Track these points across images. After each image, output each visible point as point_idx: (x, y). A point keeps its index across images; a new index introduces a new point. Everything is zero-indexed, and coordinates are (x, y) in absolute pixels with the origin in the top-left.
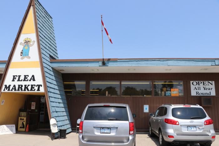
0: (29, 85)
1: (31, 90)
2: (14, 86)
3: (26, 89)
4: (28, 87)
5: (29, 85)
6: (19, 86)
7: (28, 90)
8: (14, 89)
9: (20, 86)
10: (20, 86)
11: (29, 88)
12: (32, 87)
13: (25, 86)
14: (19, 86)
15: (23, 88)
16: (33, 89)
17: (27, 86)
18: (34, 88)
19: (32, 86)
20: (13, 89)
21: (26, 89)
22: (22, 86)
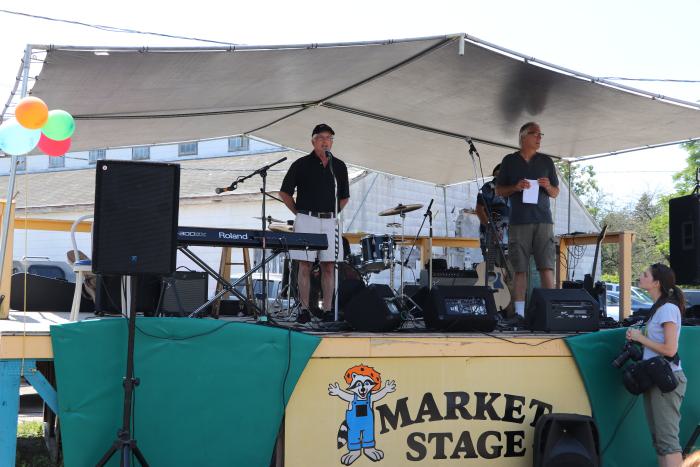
0: (495, 396)
1: (508, 417)
2: (428, 398)
3: (486, 414)
4: (495, 404)
5: (495, 396)
6: (451, 396)
7: (494, 416)
8: (426, 413)
9: (458, 400)
10: (458, 400)
11: (500, 406)
12: (509, 409)
13: (480, 396)
14: (451, 396)
15: (472, 407)
16: (515, 415)
17: (488, 399)
18: (519, 410)
19: (510, 399)
20: (422, 412)
21: (486, 414)
22: (465, 397)
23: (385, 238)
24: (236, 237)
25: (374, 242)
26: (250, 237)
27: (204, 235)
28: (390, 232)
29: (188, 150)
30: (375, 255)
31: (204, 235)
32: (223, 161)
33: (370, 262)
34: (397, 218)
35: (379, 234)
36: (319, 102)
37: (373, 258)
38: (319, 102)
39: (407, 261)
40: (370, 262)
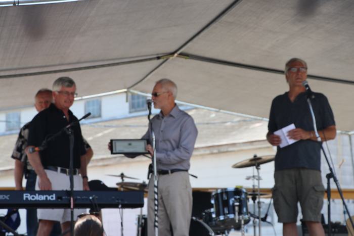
23: (238, 191)
24: (42, 198)
25: (225, 197)
26: (58, 198)
27: (7, 197)
28: (247, 185)
29: (138, 106)
30: (226, 211)
31: (7, 197)
32: (128, 122)
33: (222, 218)
34: (251, 170)
35: (231, 187)
36: (172, 54)
37: (224, 214)
38: (172, 54)
39: (266, 216)
40: (222, 218)
